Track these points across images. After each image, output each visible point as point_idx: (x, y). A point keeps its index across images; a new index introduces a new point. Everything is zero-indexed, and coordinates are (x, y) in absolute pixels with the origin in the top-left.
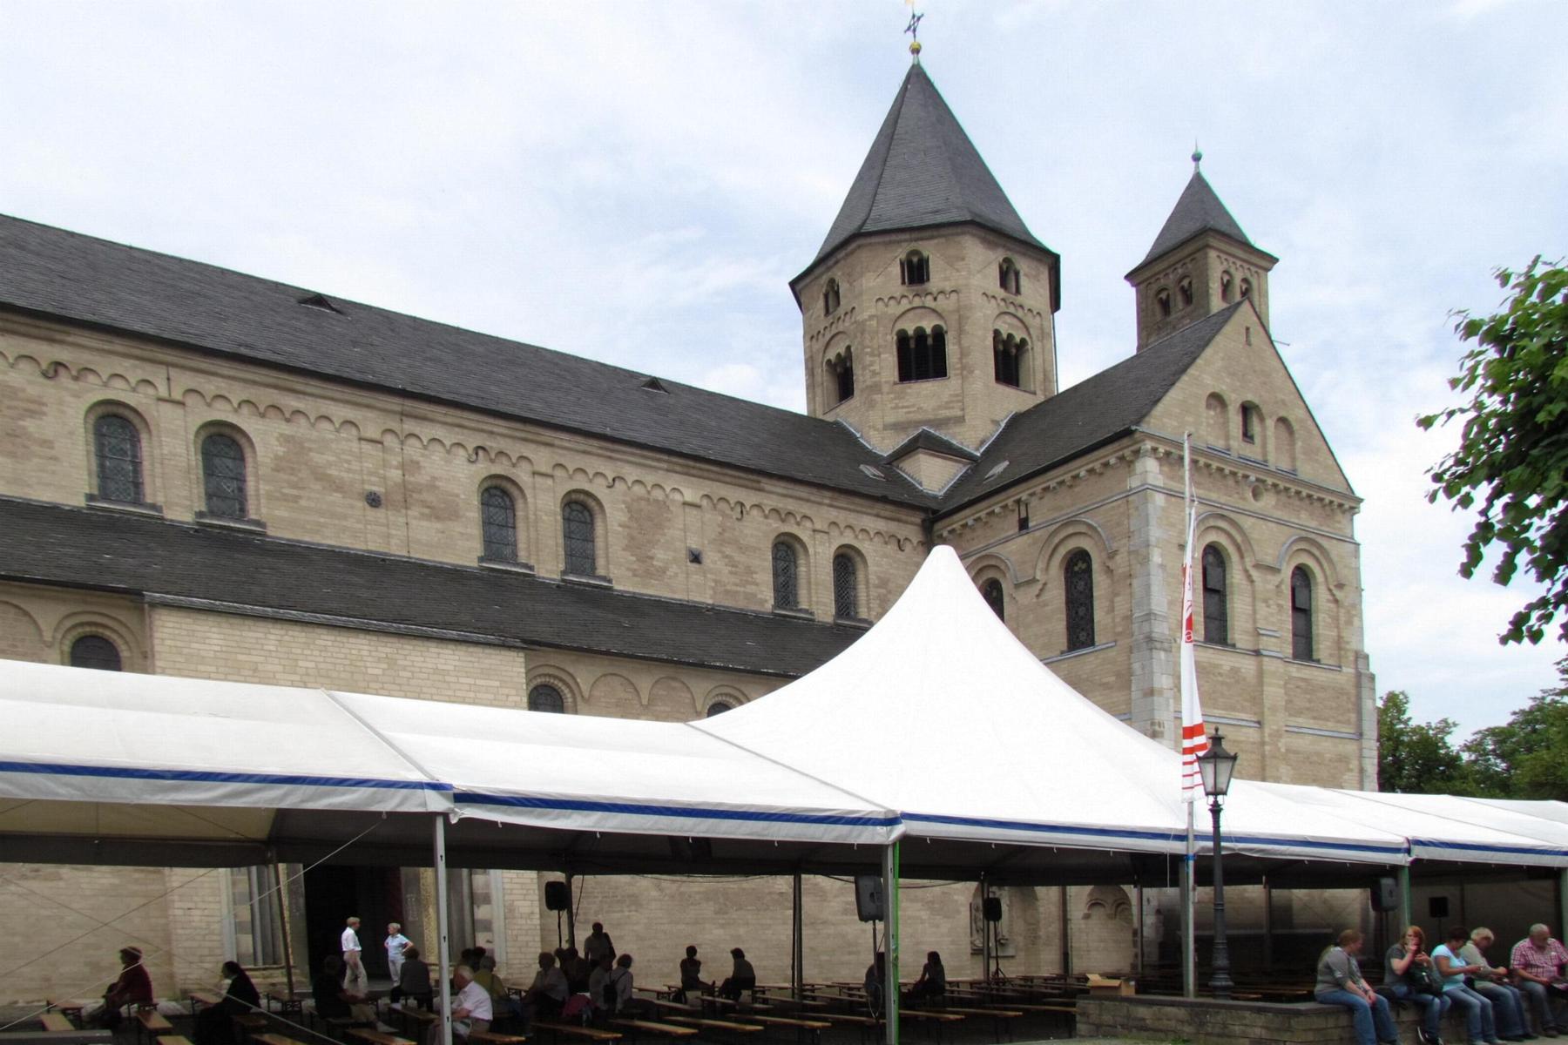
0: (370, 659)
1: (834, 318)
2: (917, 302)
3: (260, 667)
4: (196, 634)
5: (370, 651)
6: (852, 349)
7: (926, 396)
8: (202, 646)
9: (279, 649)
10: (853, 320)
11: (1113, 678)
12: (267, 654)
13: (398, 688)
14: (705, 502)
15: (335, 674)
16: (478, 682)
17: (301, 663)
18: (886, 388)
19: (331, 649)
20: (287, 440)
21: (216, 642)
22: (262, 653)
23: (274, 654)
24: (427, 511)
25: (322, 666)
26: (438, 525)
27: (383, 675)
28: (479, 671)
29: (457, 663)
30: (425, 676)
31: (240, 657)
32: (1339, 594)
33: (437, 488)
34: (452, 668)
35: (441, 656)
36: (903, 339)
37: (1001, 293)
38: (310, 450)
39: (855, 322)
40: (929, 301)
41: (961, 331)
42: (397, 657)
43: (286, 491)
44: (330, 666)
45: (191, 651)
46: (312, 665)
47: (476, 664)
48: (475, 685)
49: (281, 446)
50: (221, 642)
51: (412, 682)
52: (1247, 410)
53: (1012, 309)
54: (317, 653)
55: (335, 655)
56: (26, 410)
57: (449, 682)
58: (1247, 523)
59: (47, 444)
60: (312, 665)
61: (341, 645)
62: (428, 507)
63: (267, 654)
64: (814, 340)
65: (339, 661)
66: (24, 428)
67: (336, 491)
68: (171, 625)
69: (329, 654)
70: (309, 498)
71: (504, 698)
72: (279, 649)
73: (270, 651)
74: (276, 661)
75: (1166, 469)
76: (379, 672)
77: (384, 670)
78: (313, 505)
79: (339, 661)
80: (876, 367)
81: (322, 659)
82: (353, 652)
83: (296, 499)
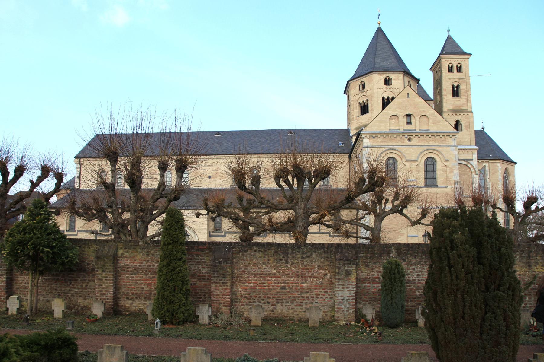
2: (362, 94)
18: (355, 119)
32: (446, 164)
37: (385, 86)
40: (365, 94)
41: (371, 100)
52: (409, 115)
53: (388, 90)
58: (403, 149)
75: (372, 140)
80: (353, 114)
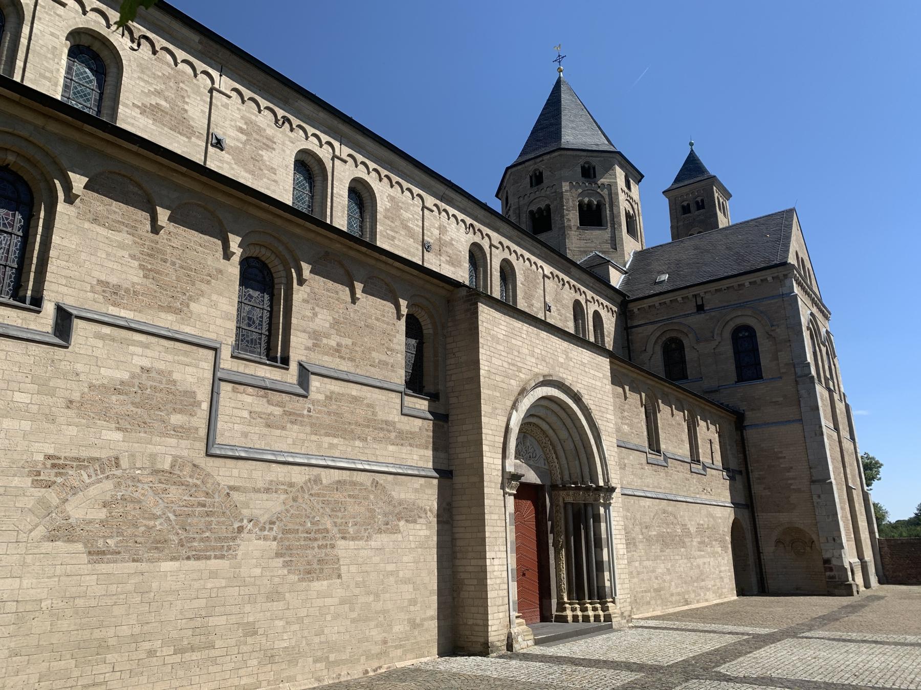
1: (538, 189)
6: (552, 207)
7: (598, 236)
10: (553, 191)
11: (782, 399)
14: (550, 276)
20: (392, 199)
24: (448, 258)
26: (453, 269)
31: (513, 341)
33: (453, 245)
36: (581, 205)
38: (401, 208)
39: (555, 192)
43: (388, 231)
49: (388, 202)
56: (264, 144)
59: (273, 170)
60: (539, 351)
62: (449, 257)
64: (521, 199)
66: (262, 156)
67: (411, 237)
70: (399, 240)
78: (400, 244)
83: (393, 238)
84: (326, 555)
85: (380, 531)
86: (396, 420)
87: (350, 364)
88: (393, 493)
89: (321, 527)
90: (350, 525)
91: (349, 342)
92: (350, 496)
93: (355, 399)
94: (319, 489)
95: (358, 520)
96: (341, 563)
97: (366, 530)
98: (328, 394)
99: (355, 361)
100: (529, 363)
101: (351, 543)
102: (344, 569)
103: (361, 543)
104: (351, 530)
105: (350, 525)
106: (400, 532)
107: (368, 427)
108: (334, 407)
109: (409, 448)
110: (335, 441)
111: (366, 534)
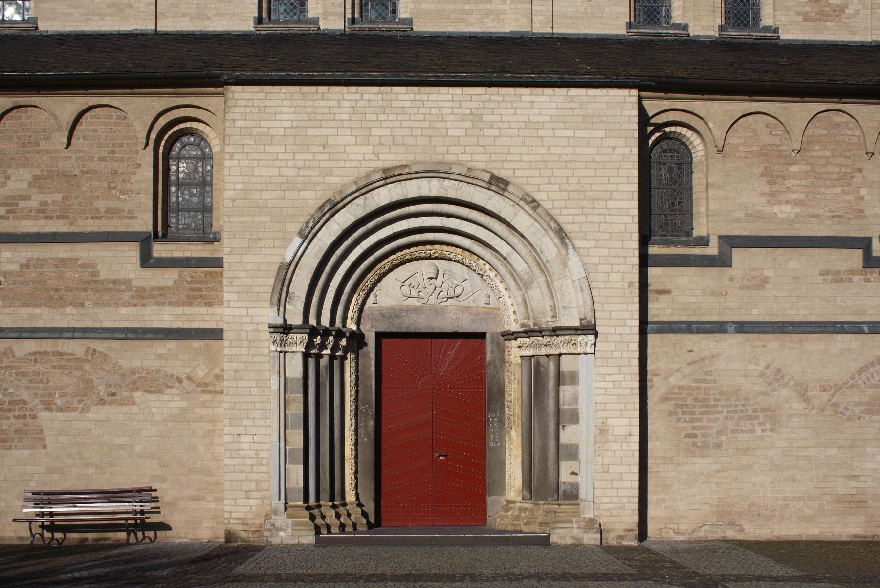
0: (452, 118)
3: (331, 141)
4: (267, 110)
5: (452, 108)
8: (272, 124)
9: (353, 117)
12: (339, 124)
13: (482, 150)
15: (410, 141)
16: (579, 133)
17: (375, 132)
19: (409, 111)
21: (284, 117)
22: (332, 124)
23: (346, 124)
25: (398, 132)
27: (466, 135)
28: (580, 119)
29: (554, 112)
30: (515, 131)
31: (310, 132)
34: (548, 119)
35: (536, 105)
42: (484, 111)
44: (407, 132)
45: (262, 130)
46: (387, 132)
47: (577, 112)
48: (574, 137)
50: (292, 117)
51: (499, 141)
54: (392, 117)
55: (412, 117)
57: (542, 138)
61: (421, 104)
63: (339, 124)
65: (417, 124)
68: (243, 103)
69: (407, 117)
71: (610, 151)
72: (353, 117)
73: (342, 120)
74: (349, 132)
76: (461, 132)
77: (467, 129)
79: (417, 124)
81: (398, 124)
82: (433, 111)
84: (26, 425)
85: (102, 402)
86: (132, 276)
87: (61, 222)
88: (121, 362)
89: (15, 398)
90: (57, 395)
91: (58, 197)
92: (54, 367)
93: (63, 262)
94: (12, 362)
95: (69, 390)
96: (46, 432)
97: (80, 402)
98: (24, 262)
99: (67, 217)
100: (352, 157)
101: (59, 414)
102: (49, 441)
103: (73, 414)
104: (59, 402)
105: (57, 395)
106: (134, 403)
107: (86, 290)
108: (33, 275)
109: (155, 308)
110: (37, 311)
111: (80, 406)
